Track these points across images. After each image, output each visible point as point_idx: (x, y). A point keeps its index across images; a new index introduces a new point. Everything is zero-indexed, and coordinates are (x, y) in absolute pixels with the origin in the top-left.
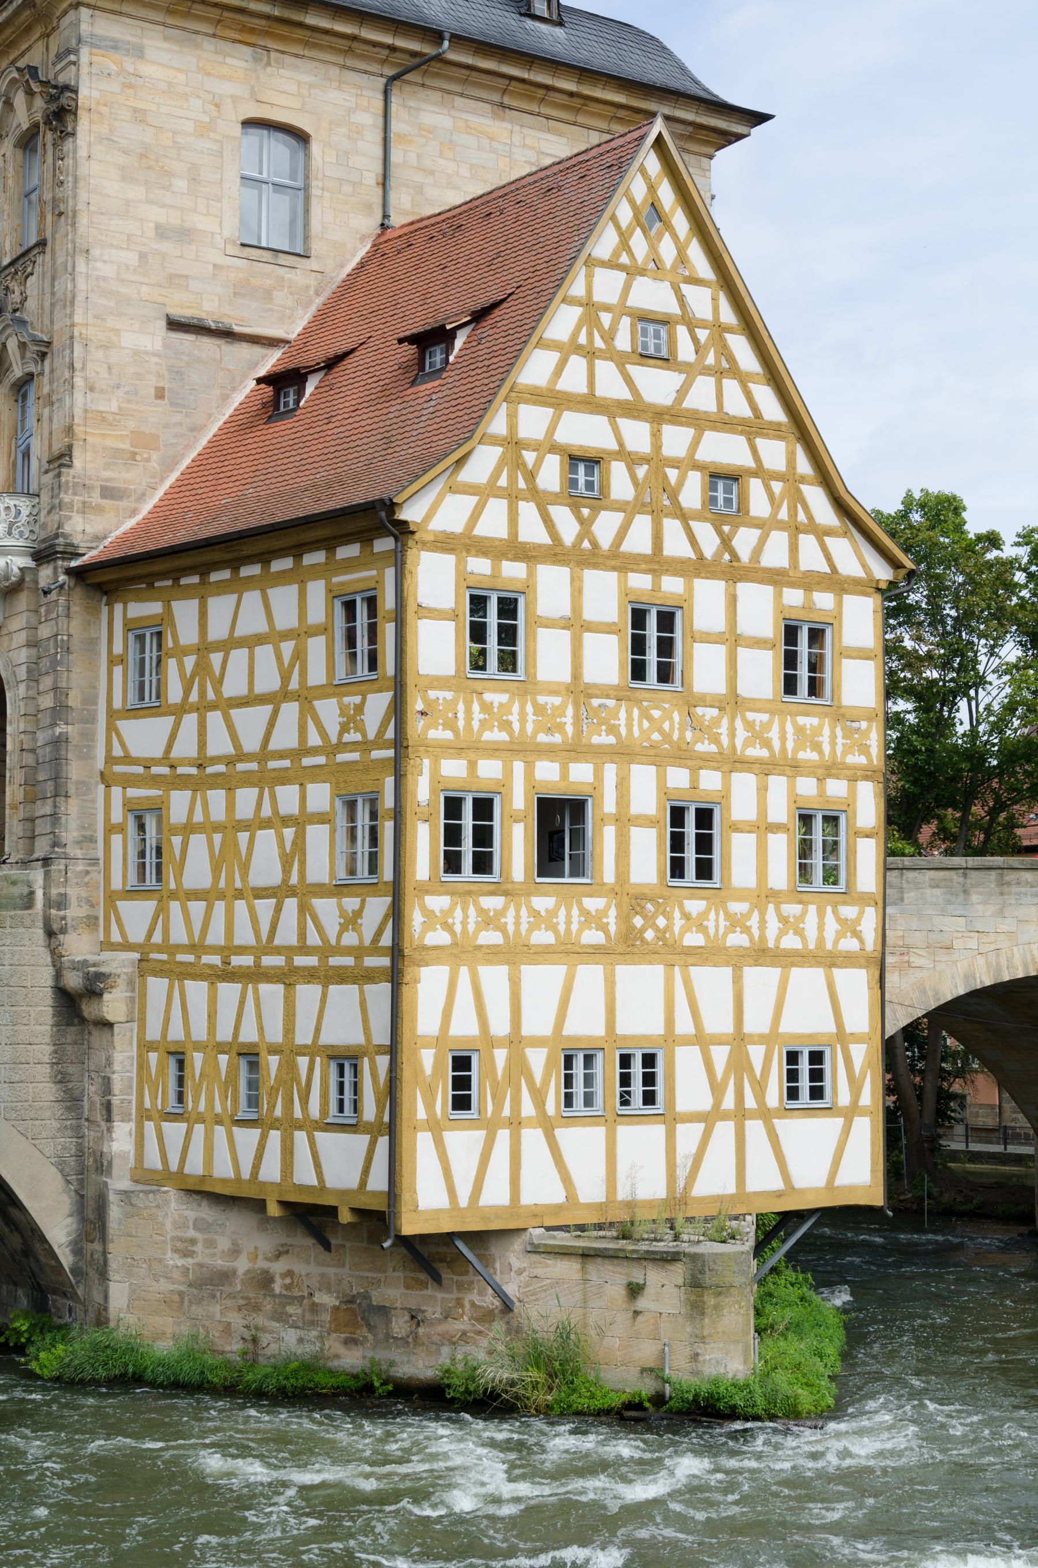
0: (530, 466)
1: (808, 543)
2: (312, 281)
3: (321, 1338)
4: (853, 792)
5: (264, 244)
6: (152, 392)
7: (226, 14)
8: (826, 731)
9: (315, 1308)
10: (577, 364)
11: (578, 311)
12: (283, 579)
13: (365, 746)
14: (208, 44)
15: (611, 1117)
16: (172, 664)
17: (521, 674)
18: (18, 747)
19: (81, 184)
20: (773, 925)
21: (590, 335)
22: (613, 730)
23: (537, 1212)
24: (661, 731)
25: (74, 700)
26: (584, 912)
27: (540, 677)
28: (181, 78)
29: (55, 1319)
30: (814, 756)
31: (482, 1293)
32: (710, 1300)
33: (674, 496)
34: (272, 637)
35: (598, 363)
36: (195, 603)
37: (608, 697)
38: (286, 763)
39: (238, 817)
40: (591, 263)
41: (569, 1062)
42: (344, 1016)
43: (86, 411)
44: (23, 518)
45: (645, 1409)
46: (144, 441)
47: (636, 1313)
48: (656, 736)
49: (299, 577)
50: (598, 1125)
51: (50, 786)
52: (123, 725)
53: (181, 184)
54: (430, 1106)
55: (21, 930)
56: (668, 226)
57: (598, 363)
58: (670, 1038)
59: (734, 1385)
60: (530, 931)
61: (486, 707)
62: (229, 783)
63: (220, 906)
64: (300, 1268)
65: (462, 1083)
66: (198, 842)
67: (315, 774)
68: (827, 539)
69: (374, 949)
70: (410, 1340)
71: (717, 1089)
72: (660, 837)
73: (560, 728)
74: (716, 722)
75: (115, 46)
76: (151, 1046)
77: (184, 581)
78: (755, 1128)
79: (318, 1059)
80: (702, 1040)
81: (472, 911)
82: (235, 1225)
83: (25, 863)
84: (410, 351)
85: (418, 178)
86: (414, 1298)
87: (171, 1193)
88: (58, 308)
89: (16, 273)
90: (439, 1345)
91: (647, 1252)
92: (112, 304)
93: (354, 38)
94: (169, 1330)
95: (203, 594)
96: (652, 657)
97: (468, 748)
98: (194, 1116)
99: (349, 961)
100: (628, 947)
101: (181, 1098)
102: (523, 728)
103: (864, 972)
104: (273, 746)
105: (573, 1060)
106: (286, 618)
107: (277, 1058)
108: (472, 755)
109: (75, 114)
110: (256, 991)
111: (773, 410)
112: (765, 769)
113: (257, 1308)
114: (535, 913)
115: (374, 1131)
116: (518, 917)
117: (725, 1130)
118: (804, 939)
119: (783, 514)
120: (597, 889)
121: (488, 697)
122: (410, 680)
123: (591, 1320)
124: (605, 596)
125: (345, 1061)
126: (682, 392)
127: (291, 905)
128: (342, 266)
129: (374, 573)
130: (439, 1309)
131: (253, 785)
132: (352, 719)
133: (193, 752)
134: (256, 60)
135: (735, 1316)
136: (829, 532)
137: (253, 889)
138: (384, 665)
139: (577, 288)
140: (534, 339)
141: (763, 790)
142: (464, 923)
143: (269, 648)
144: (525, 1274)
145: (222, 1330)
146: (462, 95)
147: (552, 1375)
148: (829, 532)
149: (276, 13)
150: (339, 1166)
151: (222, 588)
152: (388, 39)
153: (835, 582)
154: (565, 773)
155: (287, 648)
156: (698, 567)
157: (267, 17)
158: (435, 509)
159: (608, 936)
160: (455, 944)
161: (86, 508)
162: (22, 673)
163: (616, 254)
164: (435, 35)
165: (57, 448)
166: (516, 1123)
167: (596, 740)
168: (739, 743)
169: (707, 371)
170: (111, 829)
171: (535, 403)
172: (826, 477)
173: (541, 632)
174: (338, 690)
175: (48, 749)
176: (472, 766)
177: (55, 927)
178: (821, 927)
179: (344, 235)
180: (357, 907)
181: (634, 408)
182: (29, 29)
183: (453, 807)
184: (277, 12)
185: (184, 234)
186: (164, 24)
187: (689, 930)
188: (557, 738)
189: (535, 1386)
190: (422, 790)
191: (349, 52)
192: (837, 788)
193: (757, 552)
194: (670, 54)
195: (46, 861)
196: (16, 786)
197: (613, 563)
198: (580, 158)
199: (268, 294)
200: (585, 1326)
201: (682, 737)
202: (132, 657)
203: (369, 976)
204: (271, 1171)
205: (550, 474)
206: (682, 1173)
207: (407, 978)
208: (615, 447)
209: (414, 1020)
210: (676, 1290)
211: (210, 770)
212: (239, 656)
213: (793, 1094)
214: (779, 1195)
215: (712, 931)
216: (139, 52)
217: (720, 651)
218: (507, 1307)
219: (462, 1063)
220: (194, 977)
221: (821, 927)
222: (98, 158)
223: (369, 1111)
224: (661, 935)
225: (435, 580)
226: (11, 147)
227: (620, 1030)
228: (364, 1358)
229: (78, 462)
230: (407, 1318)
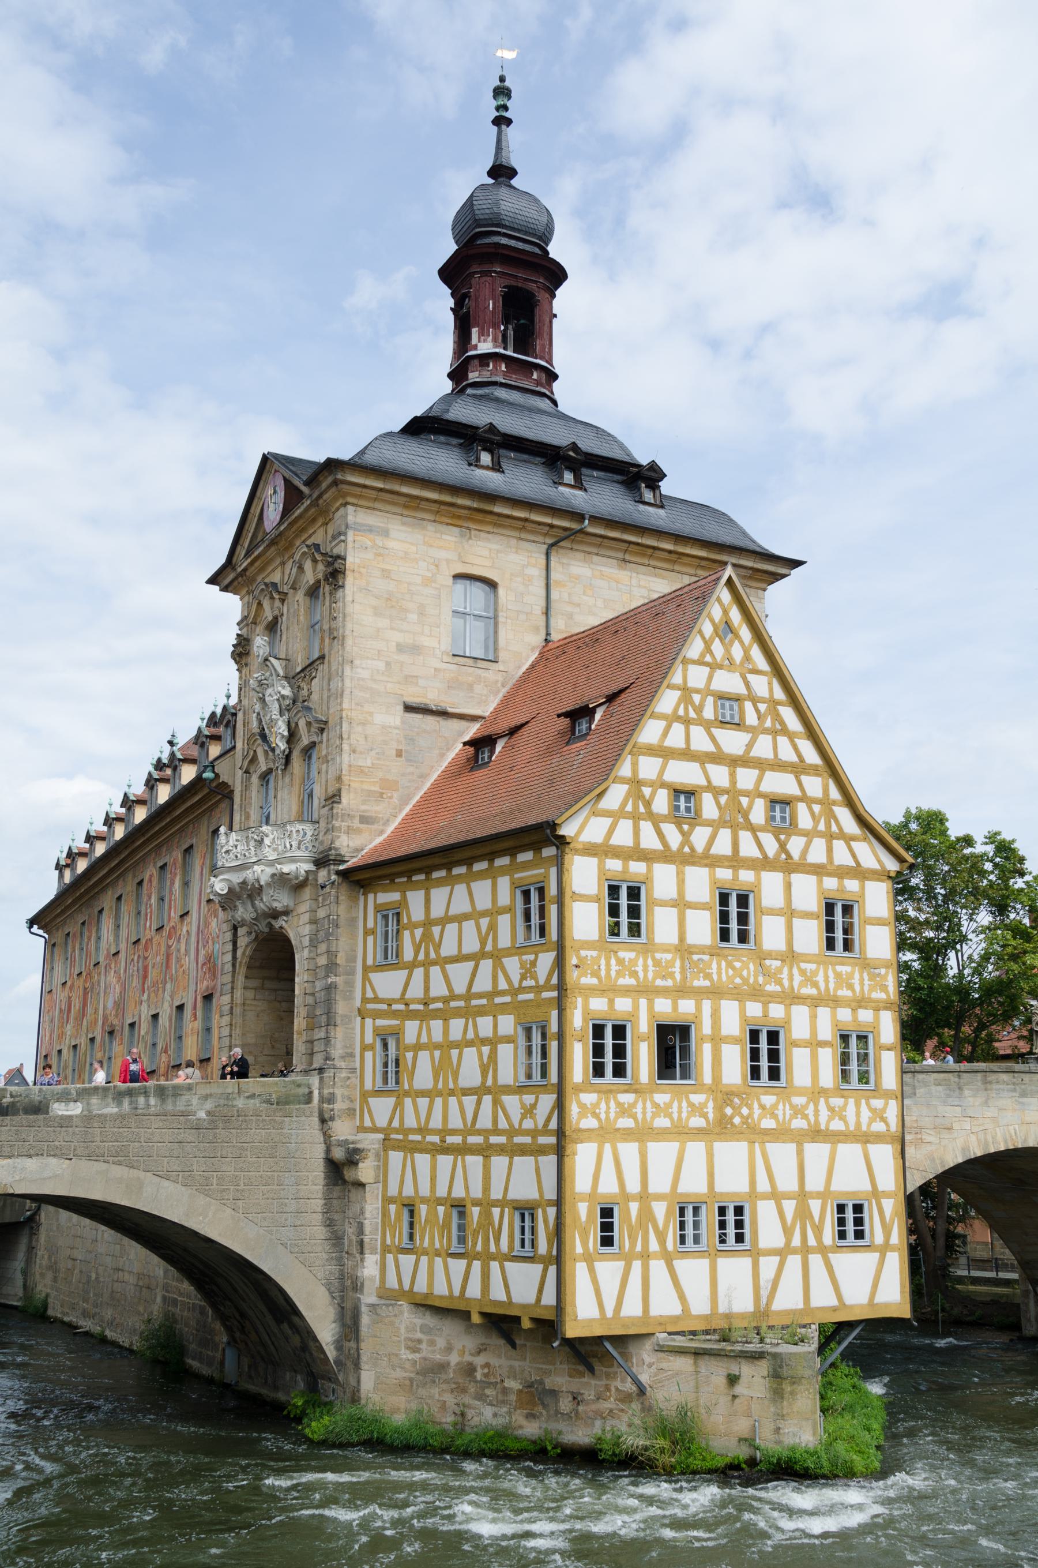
0: (647, 796)
1: (839, 845)
2: (500, 677)
3: (510, 1413)
4: (877, 1018)
5: (467, 654)
6: (394, 752)
7: (442, 507)
8: (857, 975)
9: (505, 1391)
10: (678, 729)
11: (678, 693)
12: (481, 875)
13: (537, 989)
14: (431, 527)
15: (713, 1253)
16: (406, 934)
17: (643, 938)
18: (303, 992)
19: (348, 619)
20: (824, 1113)
21: (686, 709)
22: (708, 976)
23: (662, 1321)
24: (742, 977)
25: (340, 960)
26: (691, 1105)
27: (657, 940)
28: (413, 548)
29: (323, 1397)
30: (849, 993)
31: (623, 1381)
32: (787, 1388)
33: (746, 815)
34: (474, 915)
35: (692, 727)
36: (423, 892)
37: (704, 953)
38: (484, 1001)
40: (686, 662)
41: (682, 1212)
42: (525, 1179)
43: (350, 766)
44: (308, 837)
45: (742, 1469)
46: (388, 785)
47: (734, 1397)
48: (738, 980)
49: (491, 874)
50: (704, 1257)
51: (324, 1018)
52: (375, 977)
53: (413, 617)
54: (585, 1244)
55: (303, 1118)
56: (737, 636)
57: (692, 727)
58: (754, 1195)
59: (807, 1452)
60: (653, 1118)
61: (620, 962)
62: (445, 1015)
63: (439, 1101)
64: (495, 1362)
65: (607, 1227)
66: (424, 1056)
67: (504, 1009)
68: (852, 843)
70: (573, 1415)
71: (788, 1232)
72: (743, 1052)
73: (671, 975)
74: (780, 971)
75: (370, 529)
76: (390, 1200)
77: (414, 878)
78: (816, 1261)
79: (507, 1210)
80: (776, 1196)
81: (612, 1104)
82: (448, 1329)
83: (306, 1072)
84: (565, 722)
85: (569, 609)
86: (575, 1384)
87: (404, 1305)
88: (332, 699)
90: (593, 1419)
91: (741, 1351)
92: (368, 696)
93: (526, 520)
94: (403, 1406)
95: (427, 887)
96: (734, 926)
97: (608, 990)
98: (420, 1250)
99: (528, 1140)
100: (723, 1128)
101: (411, 1237)
102: (645, 976)
103: (889, 1147)
104: (475, 989)
105: (685, 1211)
106: (483, 902)
108: (611, 996)
109: (344, 574)
110: (463, 1161)
111: (812, 756)
112: (815, 1003)
113: (464, 1391)
114: (656, 1105)
115: (546, 1261)
116: (644, 1108)
117: (794, 1262)
118: (846, 1123)
119: (822, 827)
120: (700, 1088)
121: (621, 954)
122: (568, 944)
123: (702, 1402)
124: (700, 883)
125: (525, 1210)
126: (750, 746)
128: (520, 667)
129: (543, 871)
130: (593, 1393)
132: (529, 971)
134: (462, 536)
135: (806, 1400)
136: (853, 838)
137: (462, 1089)
138: (550, 934)
139: (677, 678)
140: (649, 713)
141: (813, 1017)
142: (607, 1113)
143: (472, 922)
144: (654, 1367)
145: (440, 1407)
146: (597, 554)
147: (675, 1443)
148: (853, 838)
150: (521, 1286)
151: (440, 883)
153: (859, 872)
155: (484, 922)
156: (764, 863)
157: (469, 508)
158: (583, 827)
159: (708, 1122)
160: (601, 1127)
161: (349, 830)
162: (306, 941)
163: (703, 655)
164: (580, 517)
165: (331, 790)
166: (645, 1256)
167: (696, 983)
168: (796, 984)
169: (766, 731)
170: (364, 1048)
171: (650, 755)
172: (850, 801)
173: (658, 910)
174: (519, 951)
175: (323, 993)
176: (611, 1002)
177: (327, 1116)
178: (858, 1114)
179: (520, 648)
180: (533, 1102)
181: (718, 757)
182: (314, 520)
183: (598, 1031)
184: (475, 505)
185: (415, 649)
186: (402, 515)
187: (765, 1117)
188: (669, 983)
189: (662, 1451)
190: (577, 1020)
191: (523, 529)
192: (865, 1016)
193: (805, 852)
194: (735, 523)
195: (321, 1070)
196: (301, 1019)
197: (706, 861)
198: (677, 593)
199: (471, 687)
200: (698, 1406)
201: (756, 981)
202: (380, 930)
203: (539, 1151)
204: (474, 1290)
205: (661, 802)
206: (764, 1294)
207: (568, 1152)
208: (704, 783)
209: (573, 1182)
210: (762, 1380)
211: (432, 1007)
212: (452, 928)
213: (842, 1235)
214: (835, 1309)
215: (781, 1118)
216: (385, 533)
217: (781, 921)
218: (642, 1391)
219: (607, 1213)
220: (422, 1151)
221: (858, 1114)
222: (359, 602)
223: (543, 1247)
224: (745, 1120)
225: (584, 875)
226: (302, 595)
227: (718, 1188)
228: (540, 1428)
229: (344, 800)
230: (570, 1398)
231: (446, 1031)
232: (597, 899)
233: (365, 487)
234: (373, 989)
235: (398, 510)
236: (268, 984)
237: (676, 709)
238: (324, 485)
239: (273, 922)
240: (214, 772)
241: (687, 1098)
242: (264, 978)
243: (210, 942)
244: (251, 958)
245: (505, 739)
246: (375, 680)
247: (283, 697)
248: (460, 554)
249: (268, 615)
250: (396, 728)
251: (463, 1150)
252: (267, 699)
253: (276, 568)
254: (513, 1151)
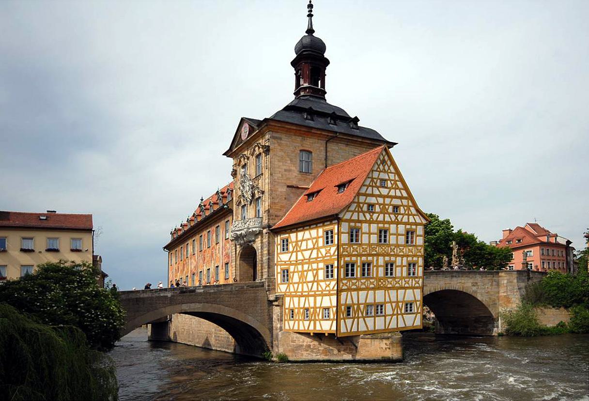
76: (287, 309)
95: (297, 231)
99: (327, 292)
120: (371, 278)
133: (295, 259)
195: (266, 279)
212: (304, 243)
238: (263, 126)
254: (323, 295)
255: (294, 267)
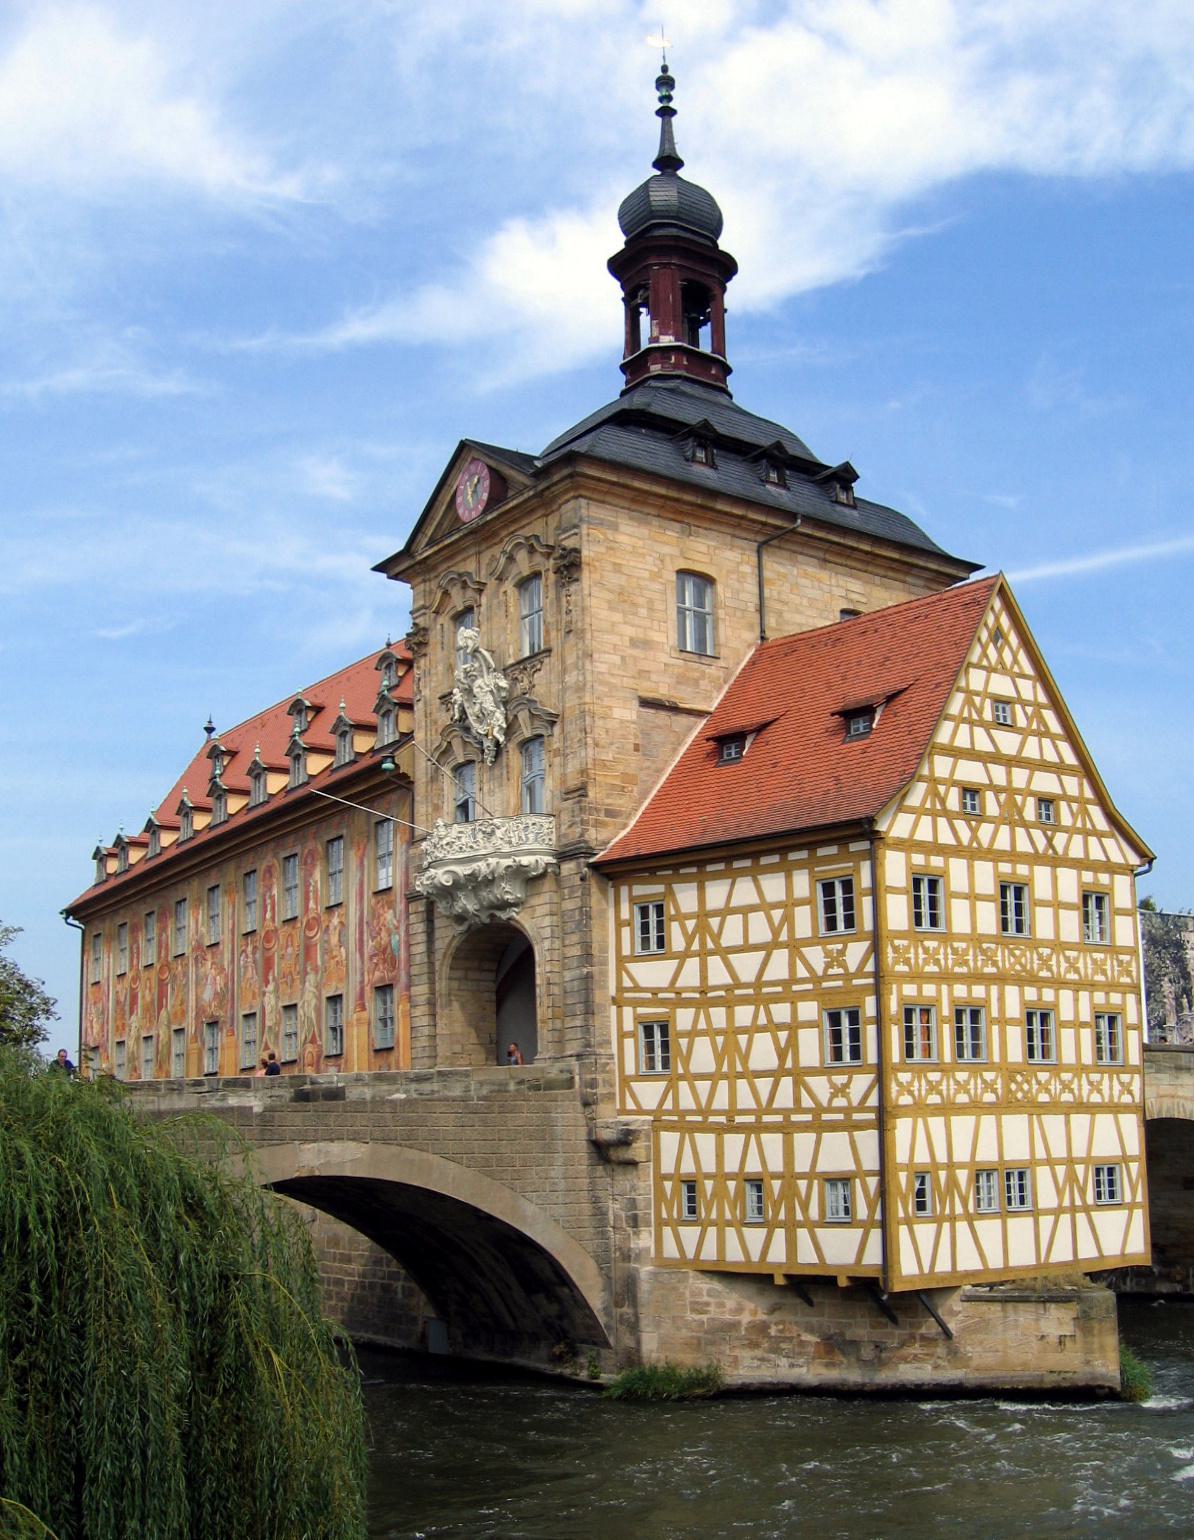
5: (689, 649)
12: (771, 869)
13: (847, 976)
14: (655, 522)
17: (941, 929)
23: (968, 1274)
25: (595, 951)
26: (984, 1081)
28: (640, 543)
34: (765, 907)
39: (737, 1025)
42: (836, 1153)
46: (629, 779)
52: (632, 967)
53: (643, 612)
60: (955, 1095)
61: (926, 950)
62: (729, 1003)
63: (723, 1085)
65: (921, 1193)
66: (703, 1046)
67: (804, 996)
69: (861, 1108)
73: (966, 963)
77: (682, 871)
79: (816, 1182)
81: (923, 1082)
85: (778, 606)
89: (525, 669)
93: (742, 517)
97: (918, 977)
100: (1005, 1105)
104: (766, 977)
107: (779, 1182)
114: (957, 1083)
115: (866, 1225)
116: (948, 1085)
121: (927, 943)
122: (884, 933)
127: (787, 1083)
128: (738, 664)
129: (851, 864)
131: (750, 1004)
133: (696, 982)
134: (683, 532)
137: (753, 1072)
142: (919, 1090)
149: (699, 502)
150: (841, 1250)
151: (717, 876)
152: (763, 518)
154: (970, 991)
155: (777, 914)
157: (691, 504)
160: (915, 1103)
161: (598, 824)
162: (547, 932)
165: (573, 783)
166: (953, 1219)
170: (622, 1035)
176: (920, 990)
177: (590, 1100)
179: (737, 643)
180: (845, 1081)
182: (532, 511)
183: (909, 1013)
185: (646, 644)
186: (629, 509)
188: (964, 970)
190: (893, 1006)
195: (579, 1056)
199: (696, 682)
205: (953, 801)
211: (710, 995)
212: (734, 922)
216: (615, 527)
222: (593, 592)
223: (862, 1212)
225: (895, 868)
229: (591, 794)
231: (730, 1017)
232: (907, 892)
233: (599, 480)
234: (632, 978)
235: (626, 505)
236: (471, 975)
237: (962, 711)
239: (499, 914)
240: (393, 762)
241: (981, 1075)
242: (467, 969)
243: (383, 934)
244: (458, 949)
245: (754, 735)
246: (613, 675)
247: (499, 688)
248: (682, 550)
249: (458, 601)
250: (634, 723)
251: (759, 1128)
252: (475, 690)
253: (468, 557)
255: (692, 1011)
